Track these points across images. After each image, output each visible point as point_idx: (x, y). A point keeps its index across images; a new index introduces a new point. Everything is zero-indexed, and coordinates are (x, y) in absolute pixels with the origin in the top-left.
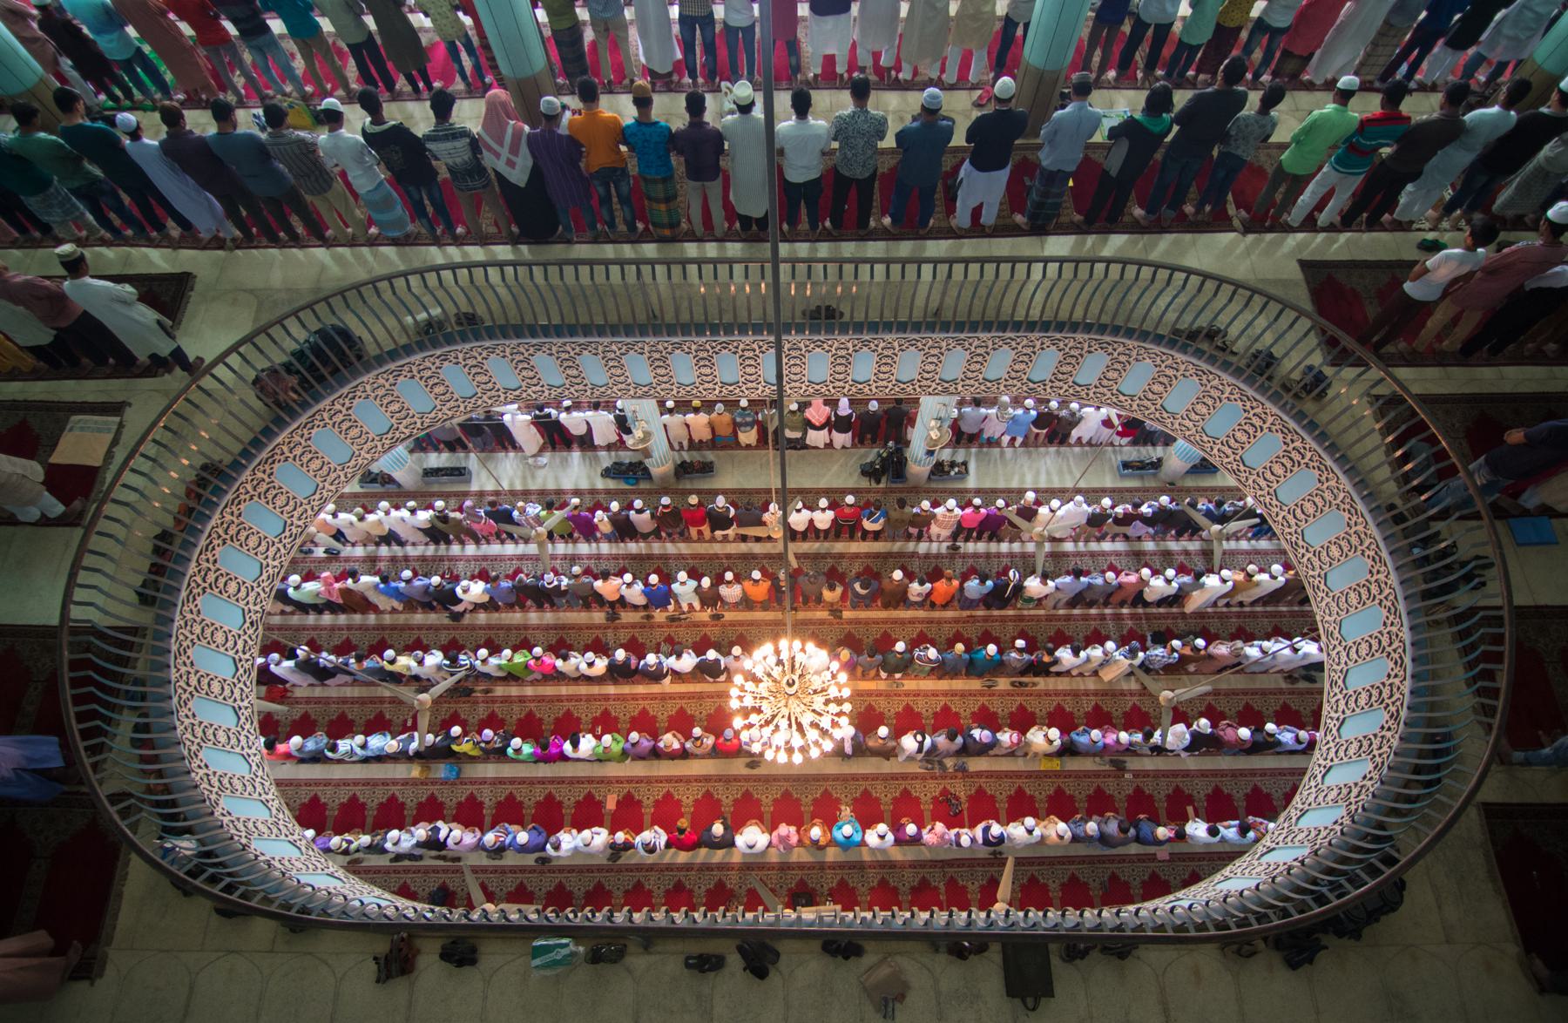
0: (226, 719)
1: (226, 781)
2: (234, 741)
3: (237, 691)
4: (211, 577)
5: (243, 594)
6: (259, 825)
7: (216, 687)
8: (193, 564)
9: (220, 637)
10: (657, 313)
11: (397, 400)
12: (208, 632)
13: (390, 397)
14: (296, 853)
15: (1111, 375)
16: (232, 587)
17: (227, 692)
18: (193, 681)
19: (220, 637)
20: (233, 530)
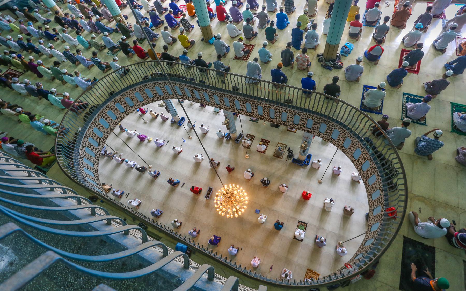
0: (95, 145)
1: (87, 156)
2: (94, 149)
3: (100, 141)
4: (104, 115)
5: (110, 121)
6: (89, 167)
7: (96, 137)
8: (101, 111)
9: (101, 128)
10: (211, 83)
11: (155, 90)
12: (99, 126)
13: (153, 90)
14: (93, 176)
15: (328, 131)
16: (108, 119)
17: (98, 139)
18: (91, 134)
19: (101, 128)
20: (112, 107)
